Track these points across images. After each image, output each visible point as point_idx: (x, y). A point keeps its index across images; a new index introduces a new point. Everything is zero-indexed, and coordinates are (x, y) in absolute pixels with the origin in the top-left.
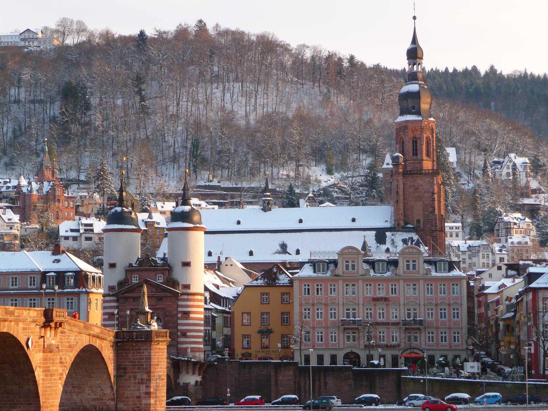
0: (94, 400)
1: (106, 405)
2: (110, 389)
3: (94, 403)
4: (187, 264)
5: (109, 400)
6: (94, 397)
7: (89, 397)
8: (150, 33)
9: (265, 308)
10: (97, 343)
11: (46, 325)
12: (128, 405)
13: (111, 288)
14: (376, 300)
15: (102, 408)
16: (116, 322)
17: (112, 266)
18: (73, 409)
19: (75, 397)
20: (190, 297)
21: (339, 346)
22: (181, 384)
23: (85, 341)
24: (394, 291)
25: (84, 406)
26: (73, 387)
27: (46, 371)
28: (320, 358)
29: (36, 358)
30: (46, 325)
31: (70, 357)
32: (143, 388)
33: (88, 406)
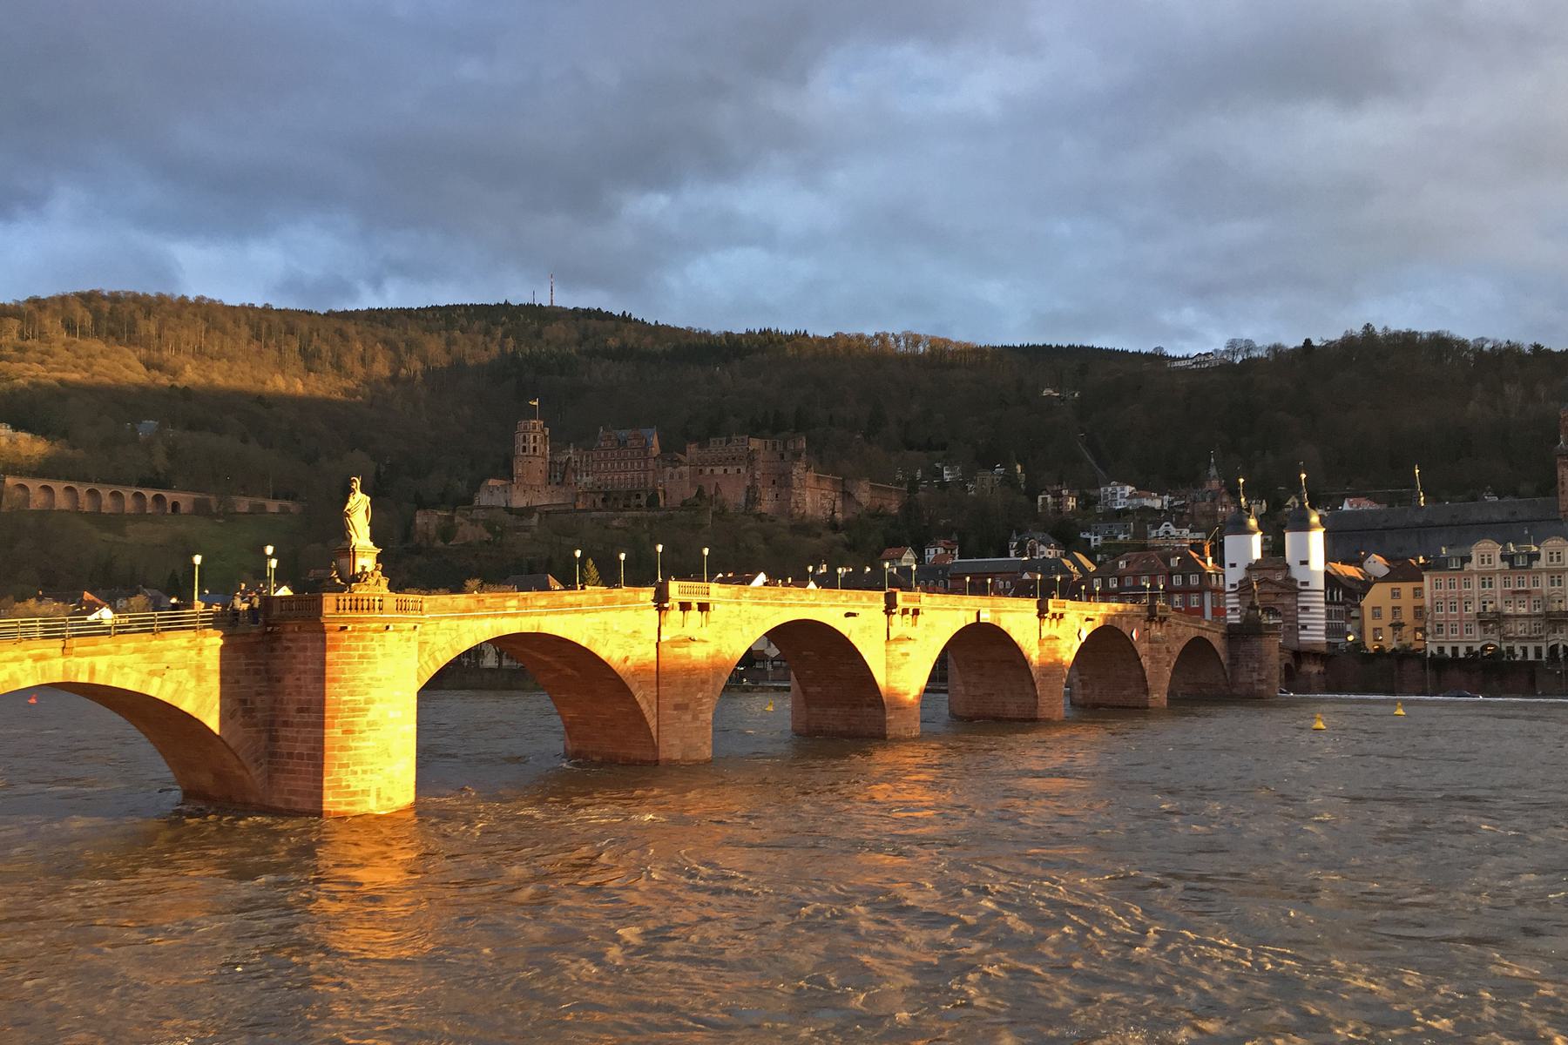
8: (1316, 343)
9: (1396, 603)
10: (1207, 635)
11: (1150, 619)
13: (1233, 586)
14: (1514, 592)
17: (1233, 565)
21: (1477, 639)
23: (1193, 633)
24: (1536, 583)
27: (1152, 658)
28: (1455, 650)
29: (1142, 648)
30: (1150, 619)
31: (1177, 647)
32: (1255, 676)
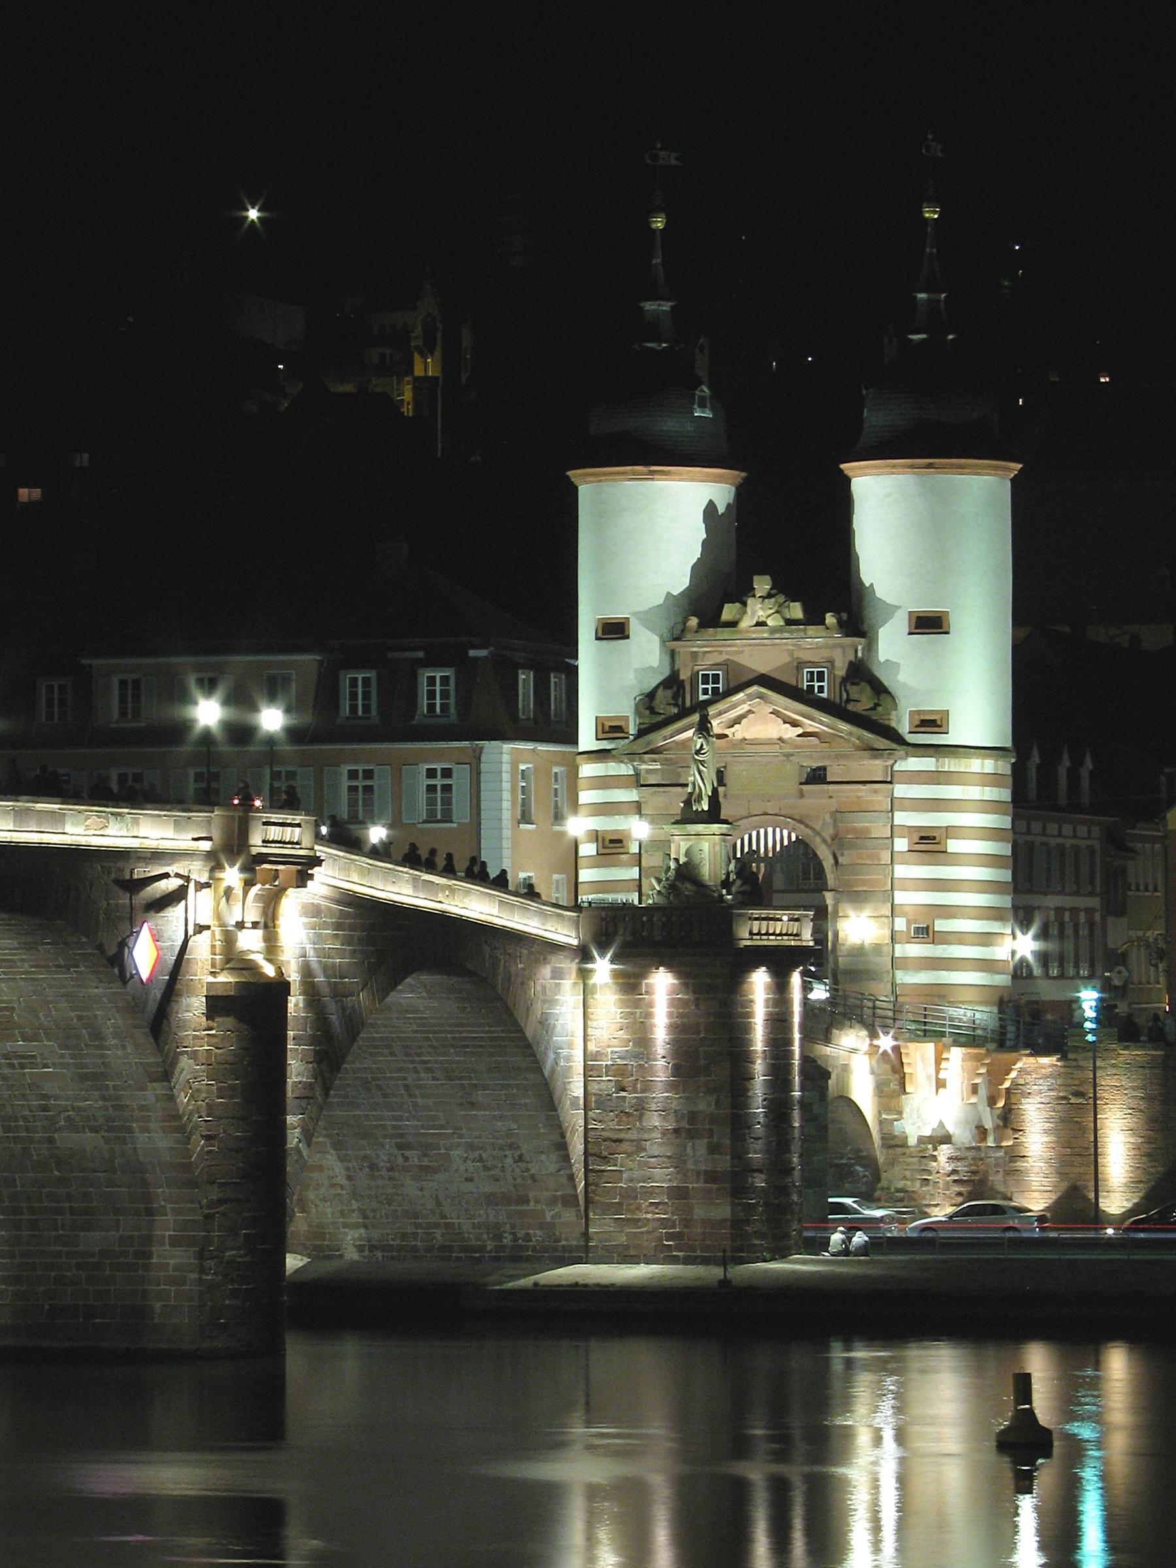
0: (490, 1200)
1: (542, 1226)
2: (554, 1157)
3: (490, 1215)
4: (929, 624)
5: (554, 1201)
6: (488, 1188)
7: (469, 1187)
12: (635, 1222)
15: (527, 1238)
16: (634, 873)
17: (613, 630)
18: (404, 1236)
19: (410, 1187)
20: (950, 764)
22: (912, 1141)
25: (448, 1226)
26: (400, 1147)
33: (467, 1225)
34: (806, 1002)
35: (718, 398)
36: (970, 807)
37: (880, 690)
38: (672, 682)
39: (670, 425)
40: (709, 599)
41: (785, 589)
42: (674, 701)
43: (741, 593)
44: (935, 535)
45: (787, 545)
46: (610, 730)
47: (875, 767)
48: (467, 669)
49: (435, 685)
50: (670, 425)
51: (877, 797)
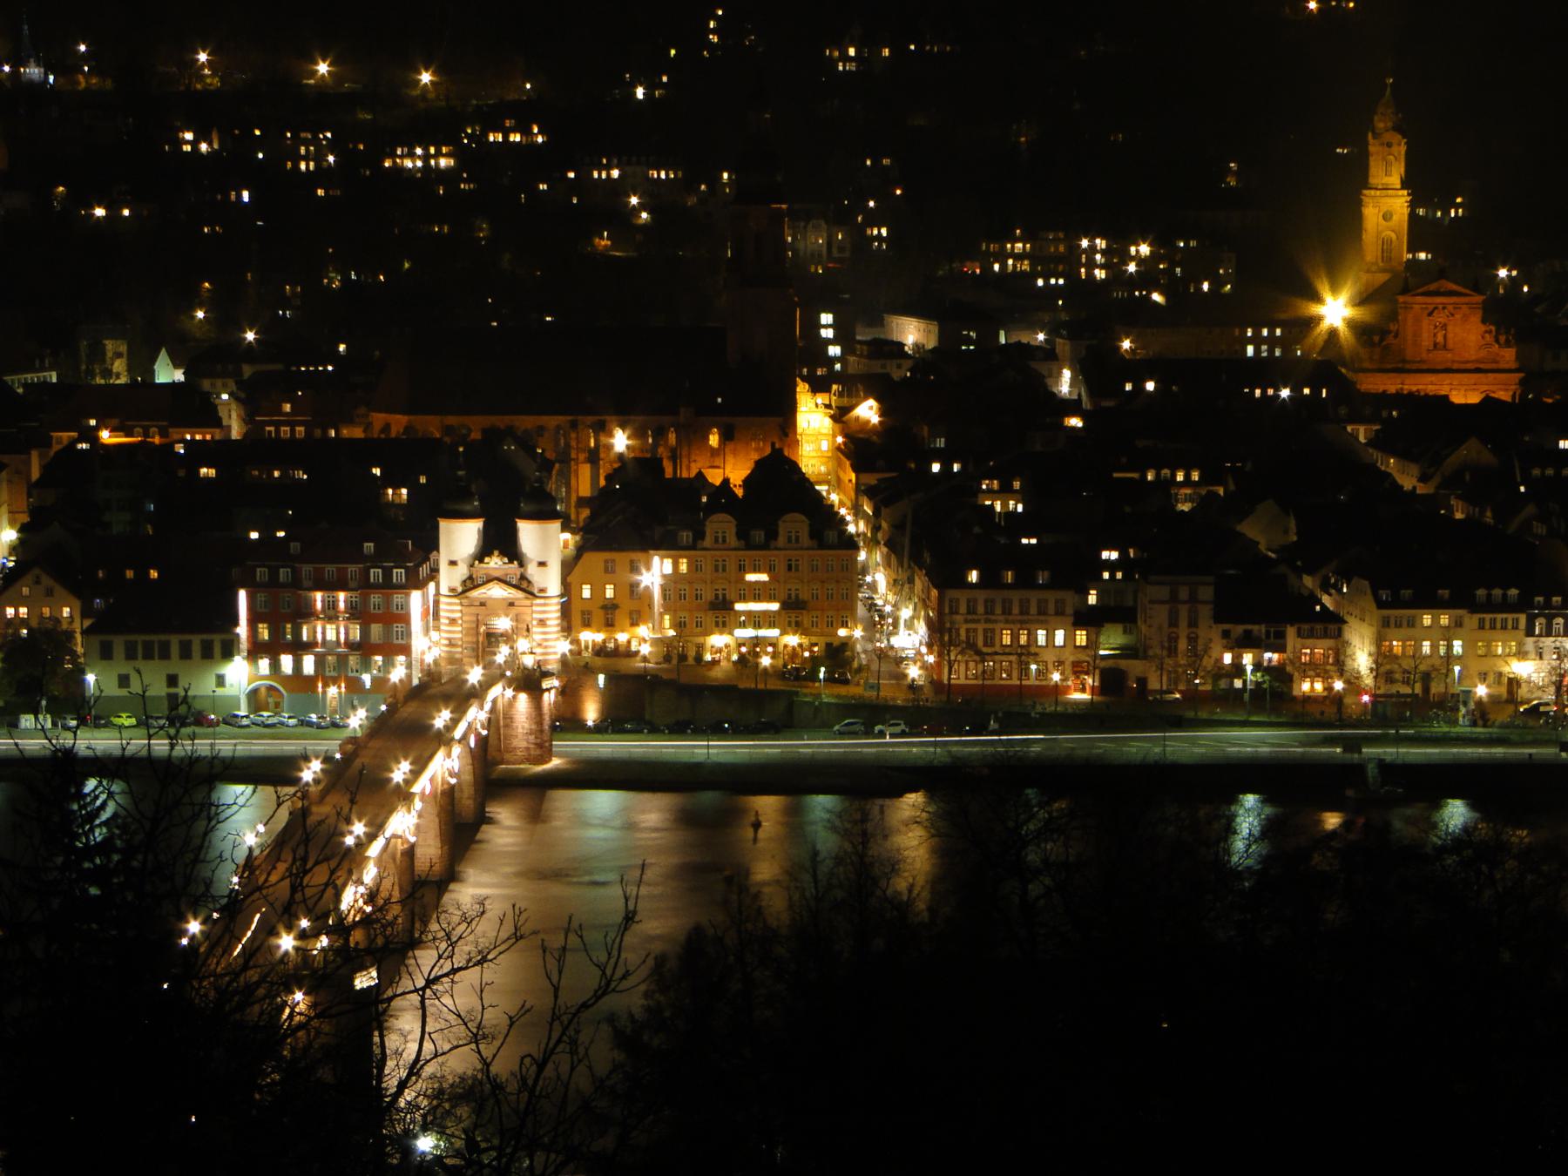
4: (542, 564)
17: (453, 563)
34: (599, 729)
35: (480, 501)
36: (552, 611)
37: (529, 582)
38: (470, 578)
39: (468, 508)
40: (482, 554)
41: (503, 554)
42: (470, 583)
43: (490, 554)
44: (544, 540)
45: (500, 540)
46: (452, 590)
47: (528, 602)
48: (407, 569)
49: (399, 574)
50: (468, 508)
51: (528, 610)
